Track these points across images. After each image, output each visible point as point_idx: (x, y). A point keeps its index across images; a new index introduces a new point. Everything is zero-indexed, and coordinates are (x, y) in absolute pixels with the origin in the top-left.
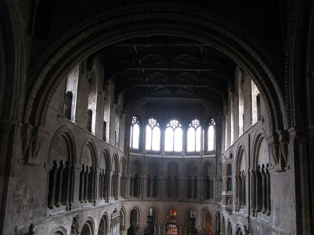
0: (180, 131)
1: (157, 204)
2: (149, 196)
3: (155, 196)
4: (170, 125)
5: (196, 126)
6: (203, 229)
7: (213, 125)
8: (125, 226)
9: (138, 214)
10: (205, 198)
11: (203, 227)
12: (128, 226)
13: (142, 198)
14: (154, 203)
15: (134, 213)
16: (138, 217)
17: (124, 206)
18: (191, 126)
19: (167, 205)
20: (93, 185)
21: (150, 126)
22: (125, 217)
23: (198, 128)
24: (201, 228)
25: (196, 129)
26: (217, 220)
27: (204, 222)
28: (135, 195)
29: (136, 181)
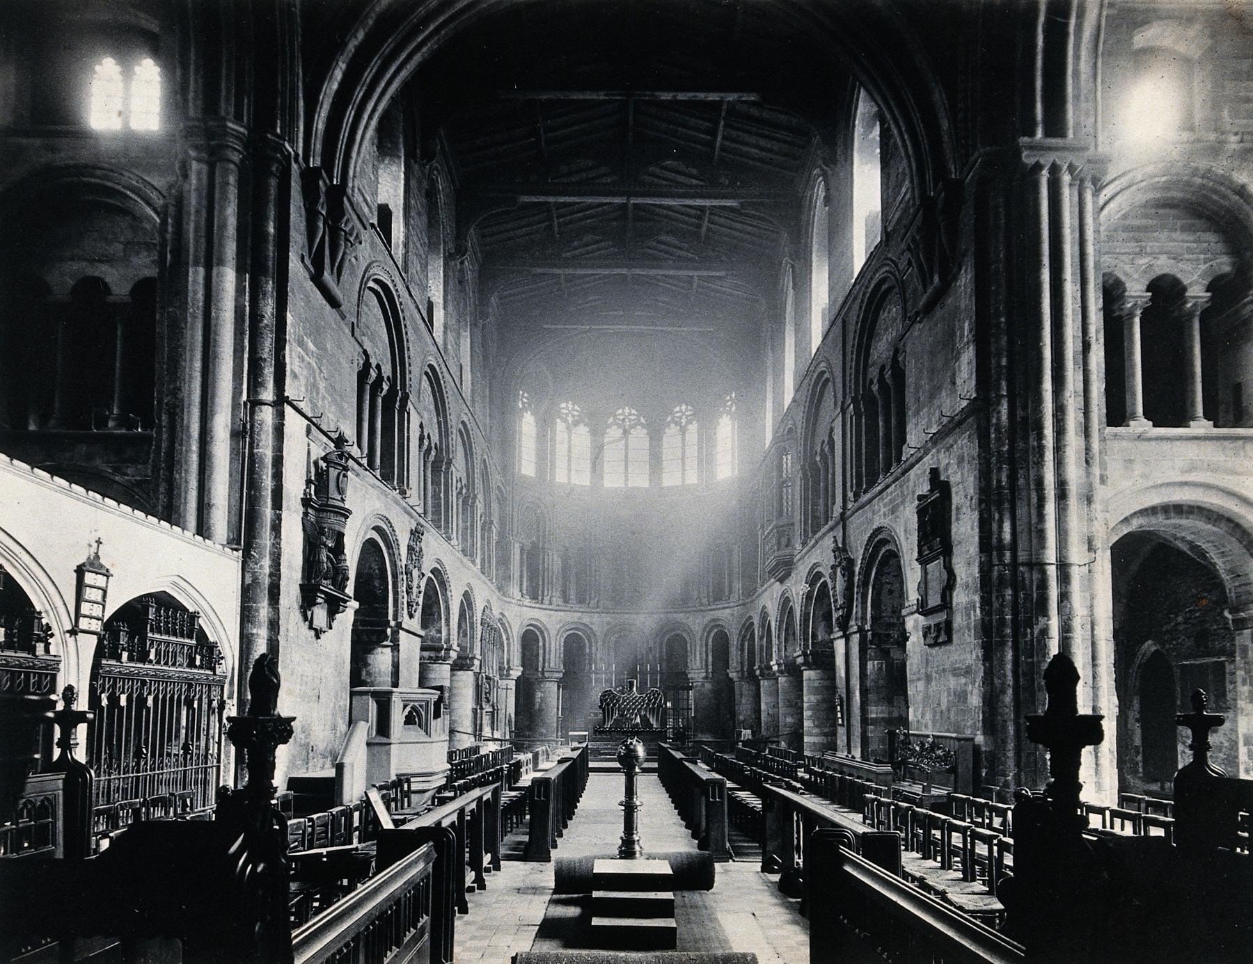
0: (639, 436)
2: (566, 601)
3: (581, 600)
4: (615, 419)
5: (684, 421)
6: (706, 678)
7: (729, 413)
8: (509, 668)
11: (707, 672)
12: (516, 672)
15: (530, 640)
16: (541, 652)
18: (673, 421)
20: (442, 495)
21: (565, 421)
23: (690, 427)
25: (683, 431)
26: (742, 645)
28: (534, 597)
29: (533, 558)
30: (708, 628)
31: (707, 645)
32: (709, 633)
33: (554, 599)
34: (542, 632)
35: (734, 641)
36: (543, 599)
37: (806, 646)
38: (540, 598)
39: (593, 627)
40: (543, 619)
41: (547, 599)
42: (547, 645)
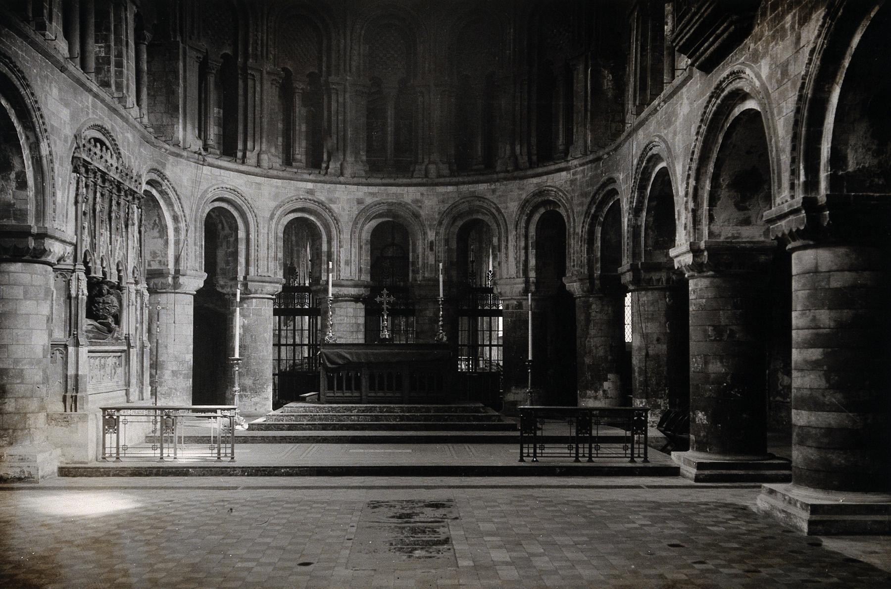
1: (322, 192)
2: (288, 161)
6: (526, 291)
9: (241, 234)
10: (534, 158)
11: (527, 282)
12: (194, 281)
13: (259, 165)
14: (311, 192)
16: (242, 247)
17: (168, 173)
19: (369, 201)
22: (177, 230)
24: (521, 287)
26: (591, 233)
27: (532, 262)
30: (529, 207)
31: (526, 237)
32: (530, 217)
33: (264, 157)
34: (243, 215)
35: (577, 227)
36: (244, 156)
37: (812, 184)
38: (240, 154)
39: (333, 206)
40: (243, 189)
41: (251, 157)
42: (252, 237)
